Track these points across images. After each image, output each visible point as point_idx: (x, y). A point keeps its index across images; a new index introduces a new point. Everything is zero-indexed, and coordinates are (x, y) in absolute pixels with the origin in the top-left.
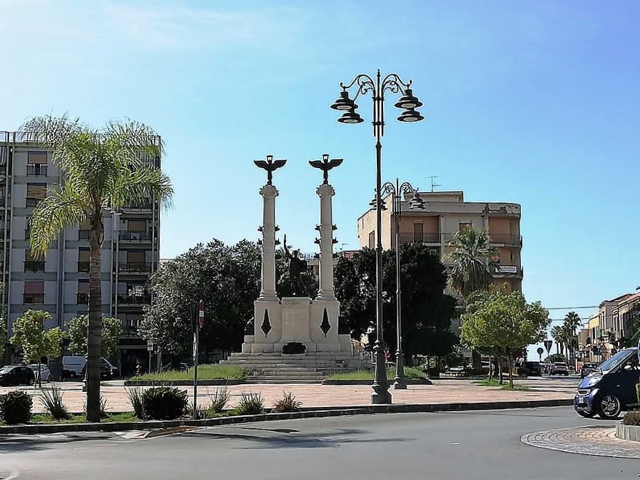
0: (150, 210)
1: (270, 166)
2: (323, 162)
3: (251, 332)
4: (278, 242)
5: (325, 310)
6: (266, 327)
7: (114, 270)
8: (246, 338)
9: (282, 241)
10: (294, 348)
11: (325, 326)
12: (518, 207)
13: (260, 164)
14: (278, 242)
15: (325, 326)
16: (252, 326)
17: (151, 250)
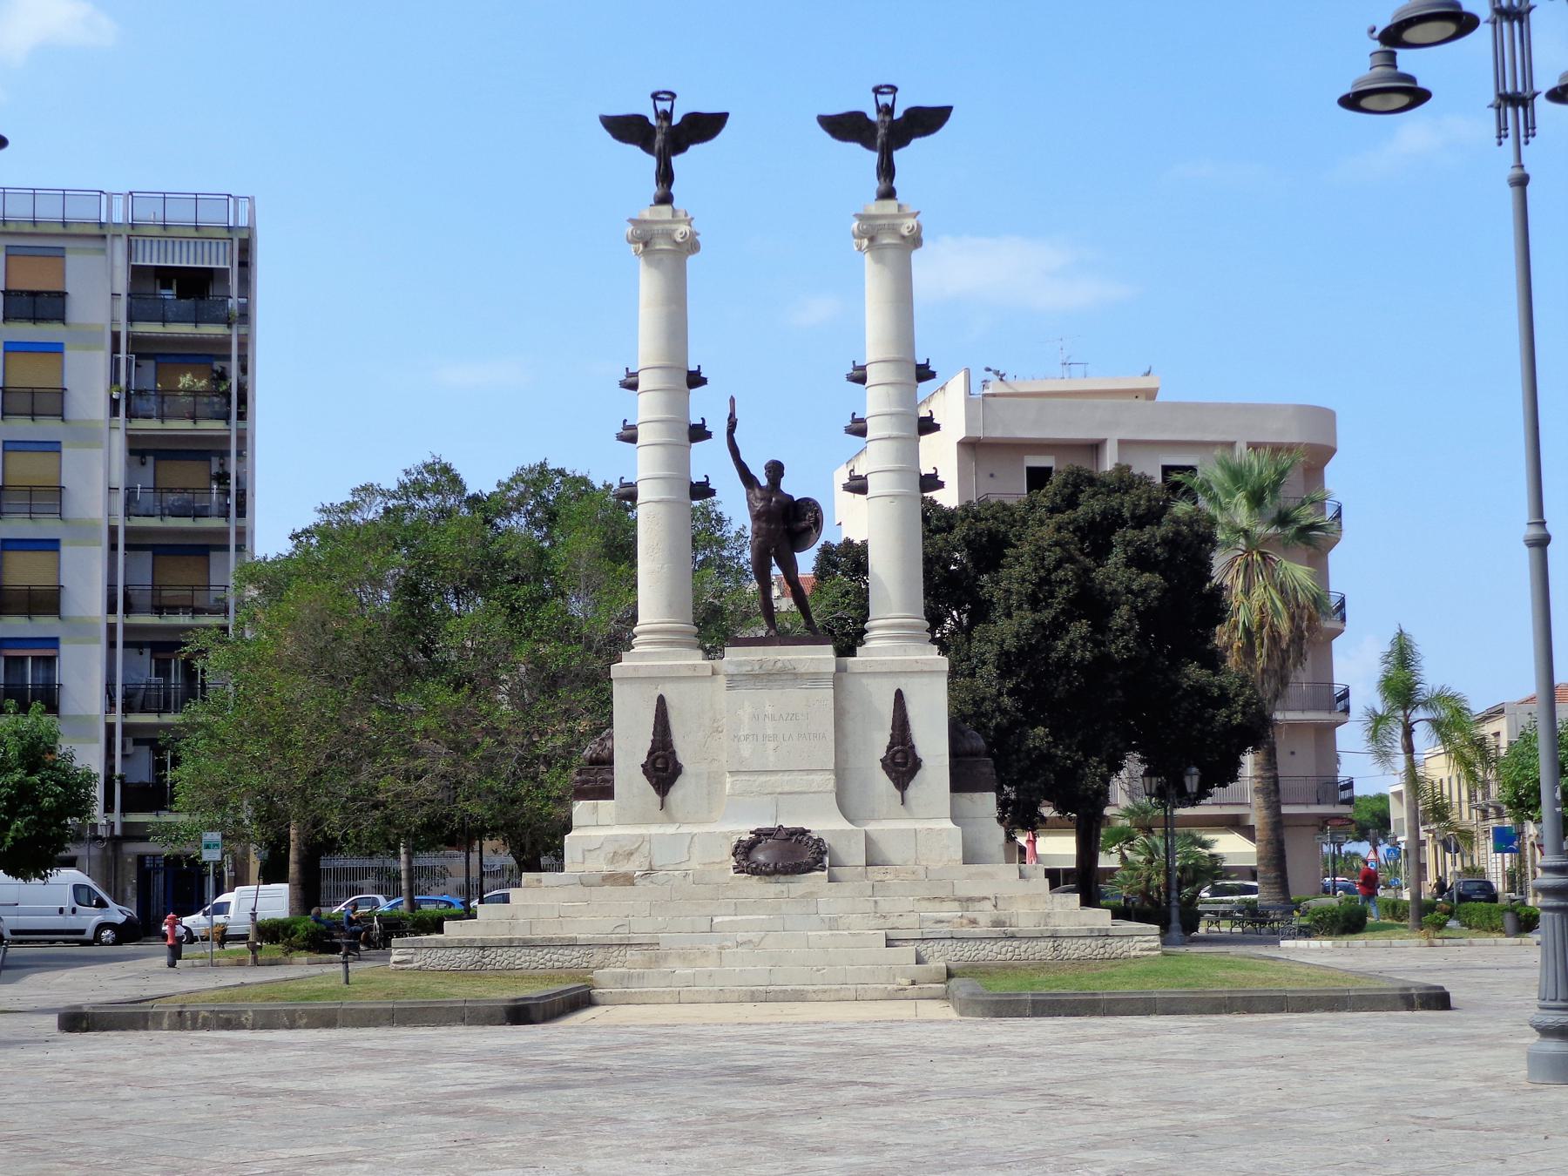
0: (220, 425)
1: (665, 135)
2: (873, 115)
3: (606, 792)
4: (699, 433)
5: (899, 695)
6: (663, 769)
7: (112, 609)
8: (581, 810)
9: (718, 427)
10: (784, 855)
11: (902, 764)
12: (1327, 418)
13: (626, 128)
14: (699, 433)
15: (902, 764)
16: (605, 762)
17: (226, 548)
